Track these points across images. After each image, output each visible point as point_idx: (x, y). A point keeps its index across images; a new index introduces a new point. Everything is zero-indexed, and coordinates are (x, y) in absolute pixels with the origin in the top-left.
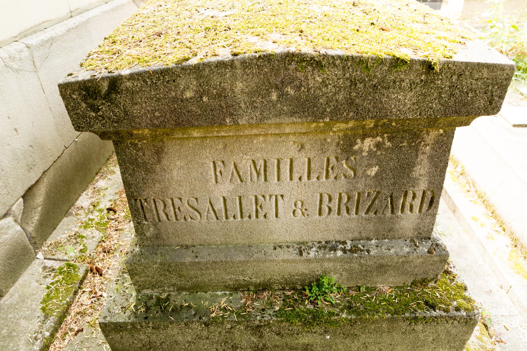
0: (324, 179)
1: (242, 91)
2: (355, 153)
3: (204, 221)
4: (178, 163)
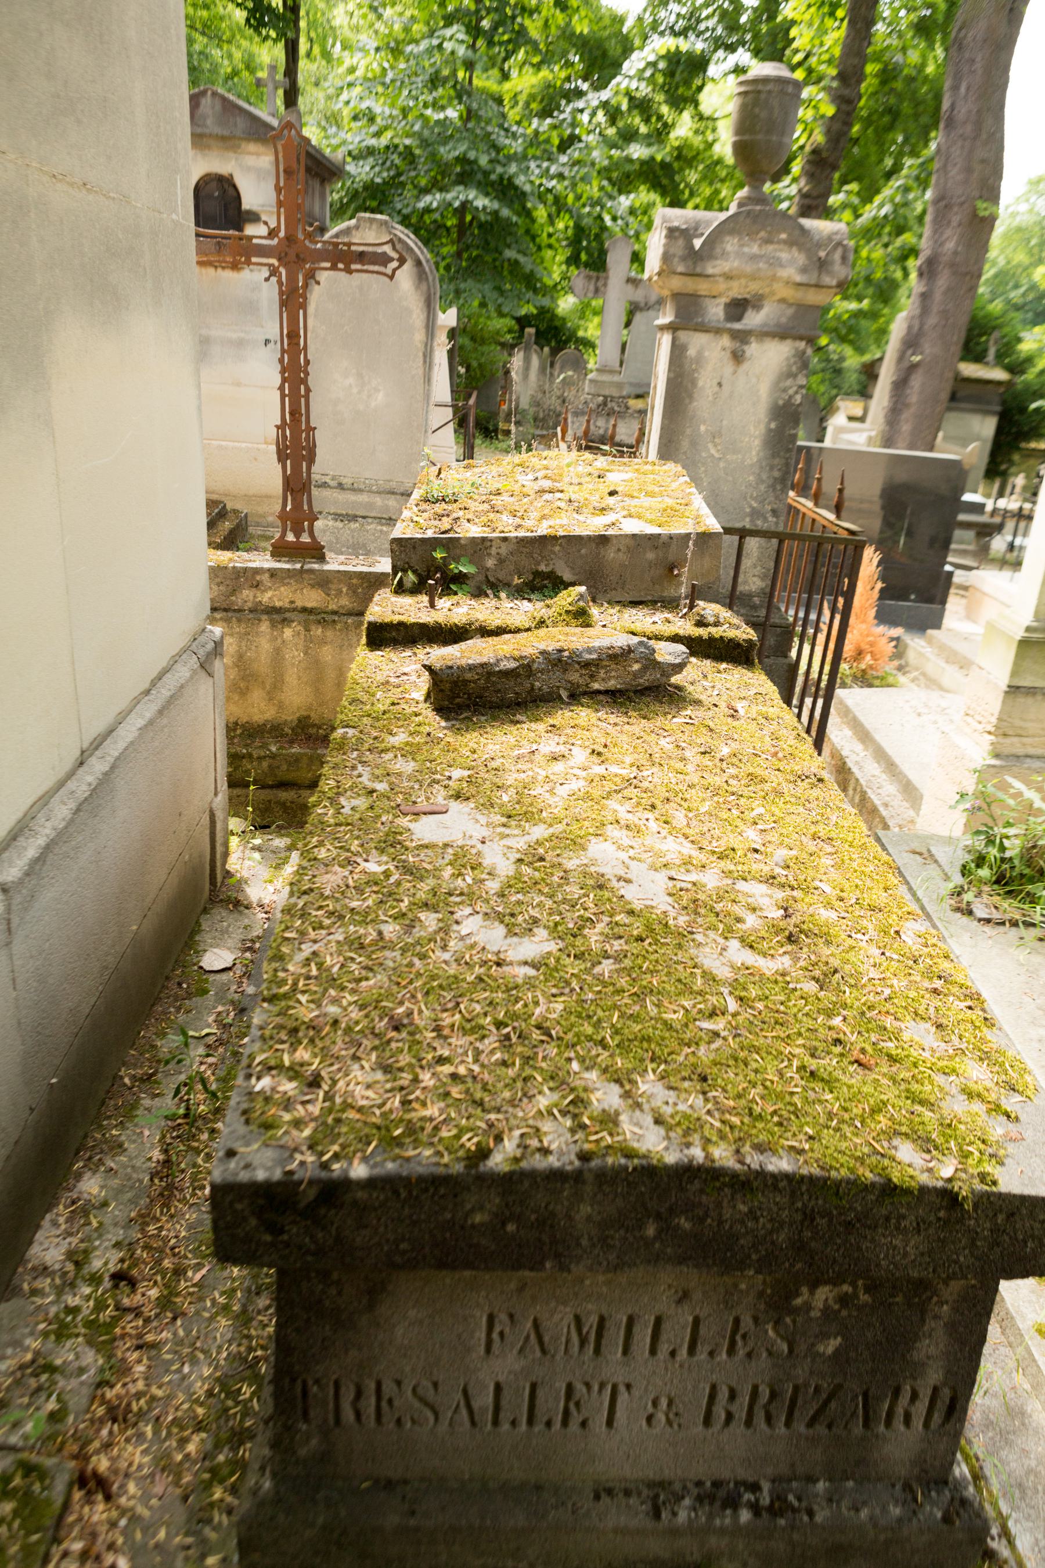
0: (724, 1356)
1: (589, 1219)
2: (794, 1311)
3: (443, 1427)
4: (412, 1313)
